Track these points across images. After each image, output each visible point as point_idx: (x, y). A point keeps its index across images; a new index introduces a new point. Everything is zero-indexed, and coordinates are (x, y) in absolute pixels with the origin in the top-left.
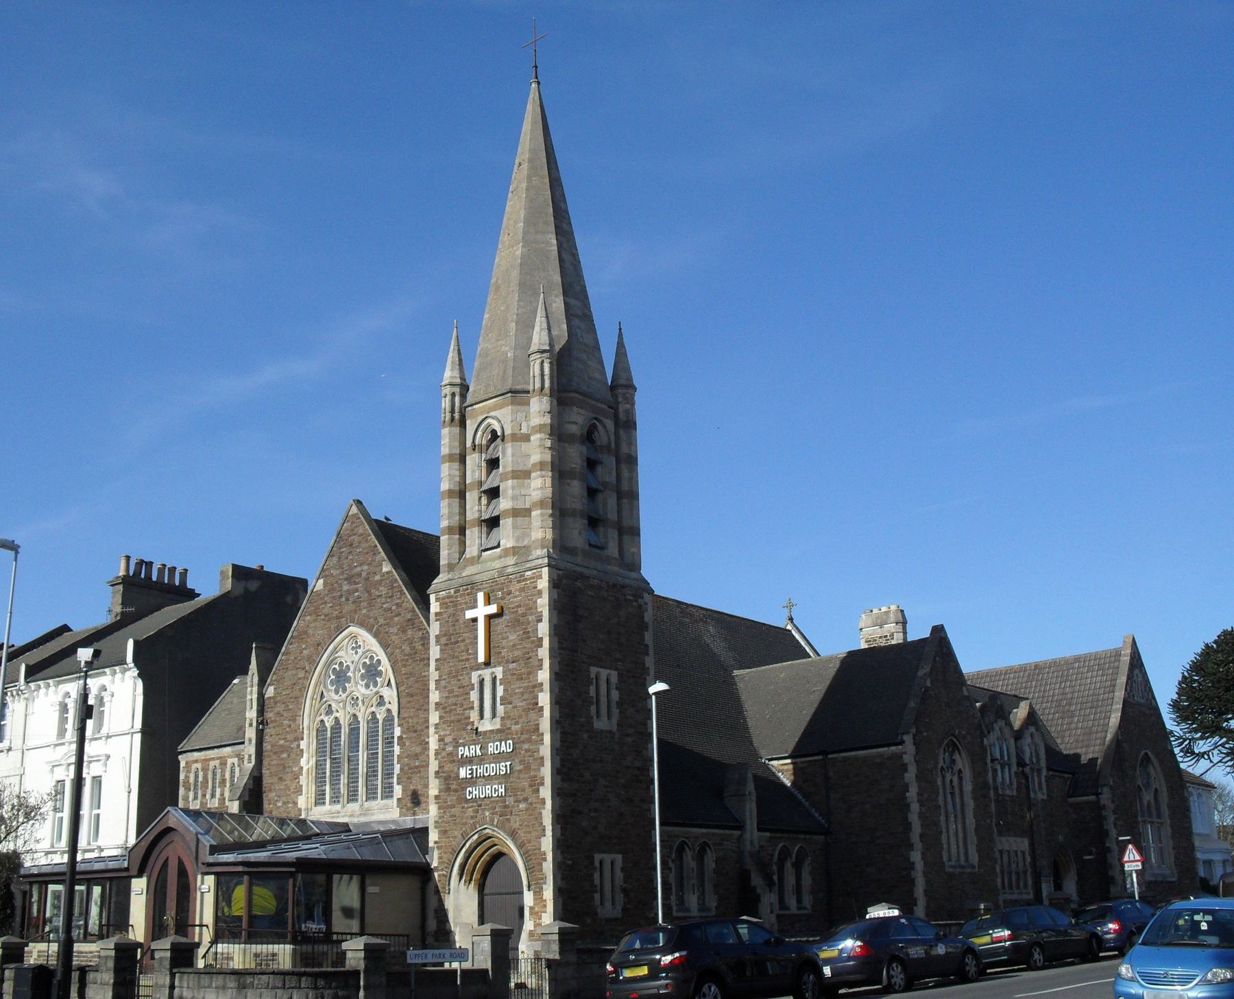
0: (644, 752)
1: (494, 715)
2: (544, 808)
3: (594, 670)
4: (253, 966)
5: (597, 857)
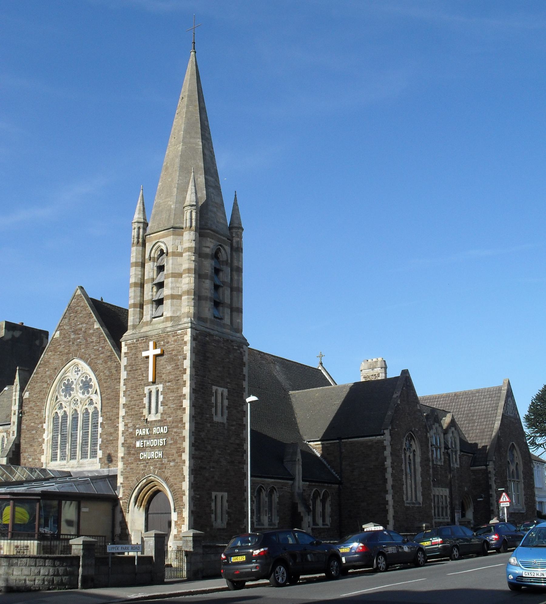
0: (241, 435)
1: (157, 412)
3: (214, 388)
4: (15, 553)
5: (214, 494)
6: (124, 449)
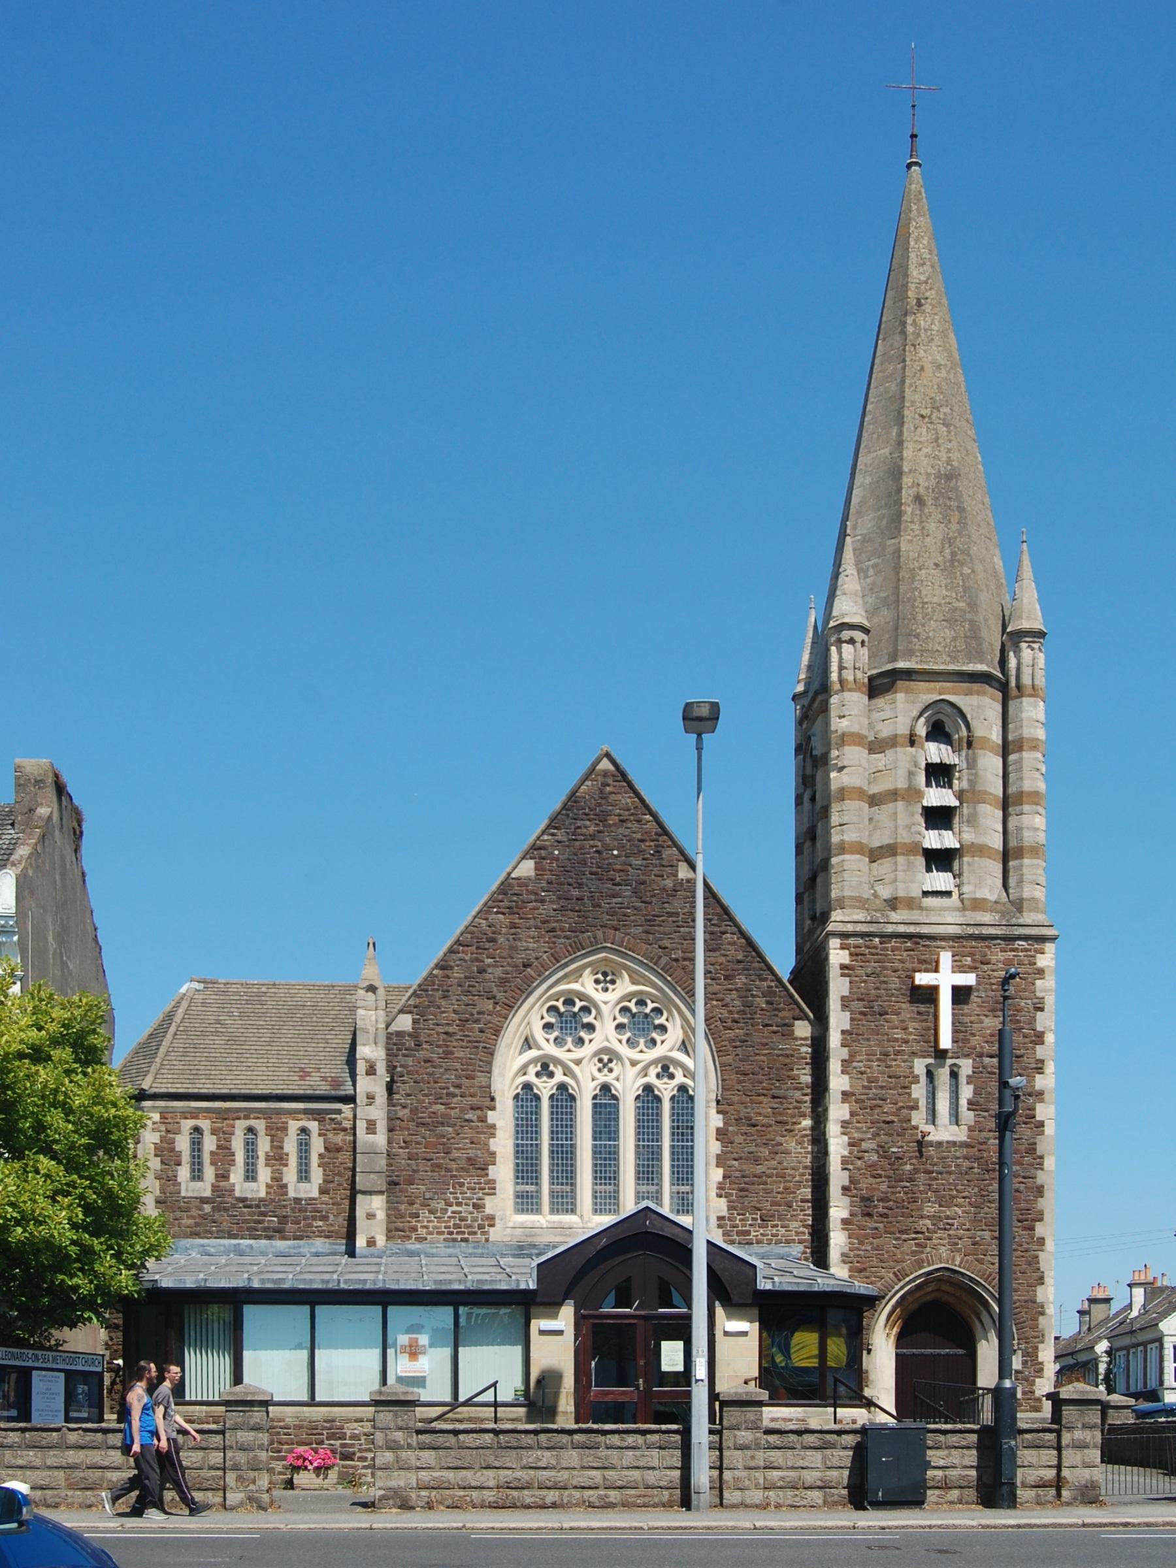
2: (1042, 1250)
6: (852, 1202)
